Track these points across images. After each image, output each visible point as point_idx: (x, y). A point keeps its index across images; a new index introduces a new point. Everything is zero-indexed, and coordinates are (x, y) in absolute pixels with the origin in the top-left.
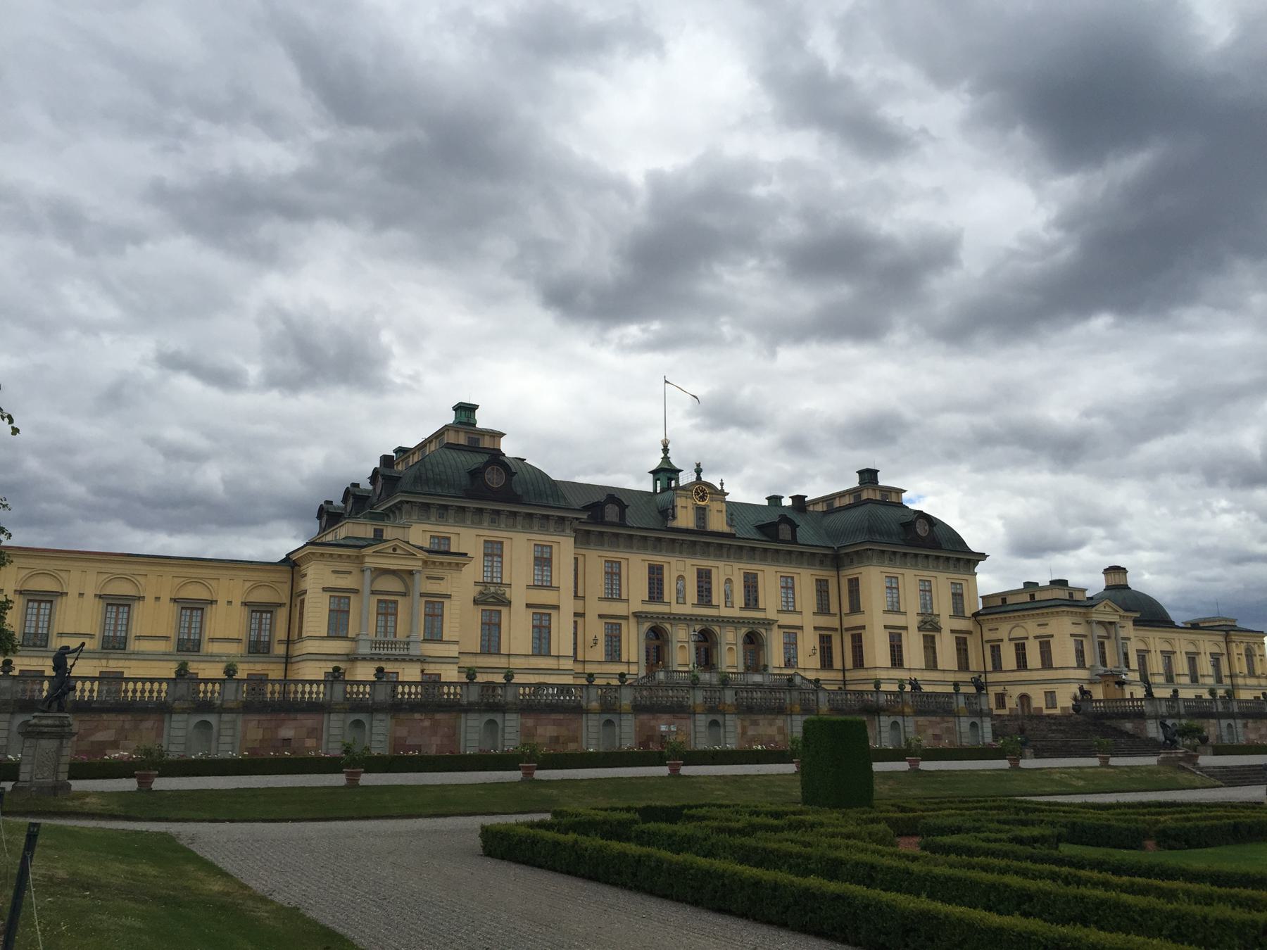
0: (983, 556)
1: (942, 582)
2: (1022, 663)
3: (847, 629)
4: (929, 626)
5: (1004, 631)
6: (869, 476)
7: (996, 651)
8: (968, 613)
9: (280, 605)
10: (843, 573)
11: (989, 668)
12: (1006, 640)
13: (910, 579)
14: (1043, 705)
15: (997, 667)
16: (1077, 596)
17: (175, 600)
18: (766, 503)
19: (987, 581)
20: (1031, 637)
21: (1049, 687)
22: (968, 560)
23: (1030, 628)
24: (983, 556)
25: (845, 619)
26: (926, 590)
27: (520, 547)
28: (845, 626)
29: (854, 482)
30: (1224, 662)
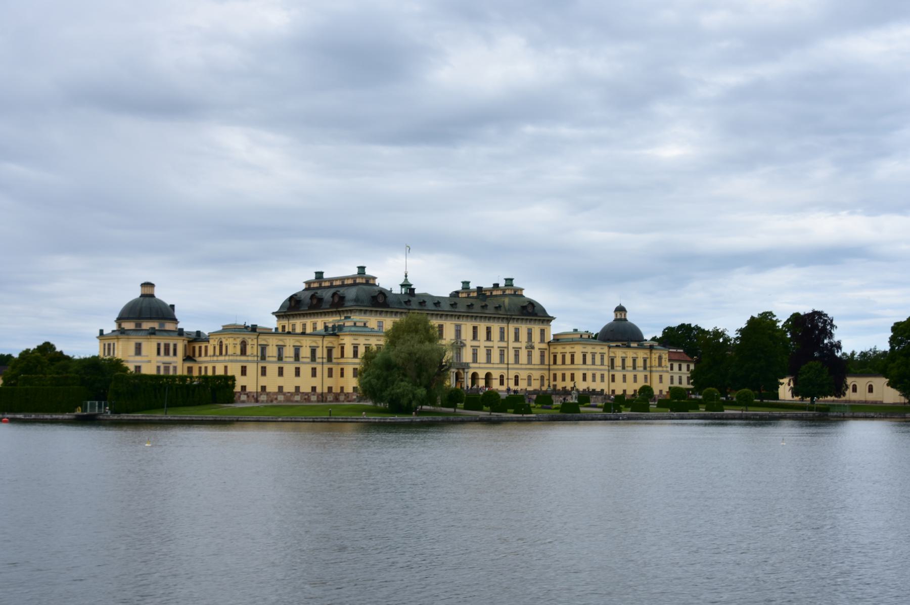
0: (553, 318)
1: (536, 329)
2: (564, 363)
4: (530, 347)
5: (559, 349)
7: (555, 357)
8: (546, 341)
11: (552, 362)
13: (524, 328)
15: (555, 363)
19: (555, 328)
22: (548, 319)
23: (568, 349)
24: (553, 318)
29: (502, 284)
30: (648, 361)
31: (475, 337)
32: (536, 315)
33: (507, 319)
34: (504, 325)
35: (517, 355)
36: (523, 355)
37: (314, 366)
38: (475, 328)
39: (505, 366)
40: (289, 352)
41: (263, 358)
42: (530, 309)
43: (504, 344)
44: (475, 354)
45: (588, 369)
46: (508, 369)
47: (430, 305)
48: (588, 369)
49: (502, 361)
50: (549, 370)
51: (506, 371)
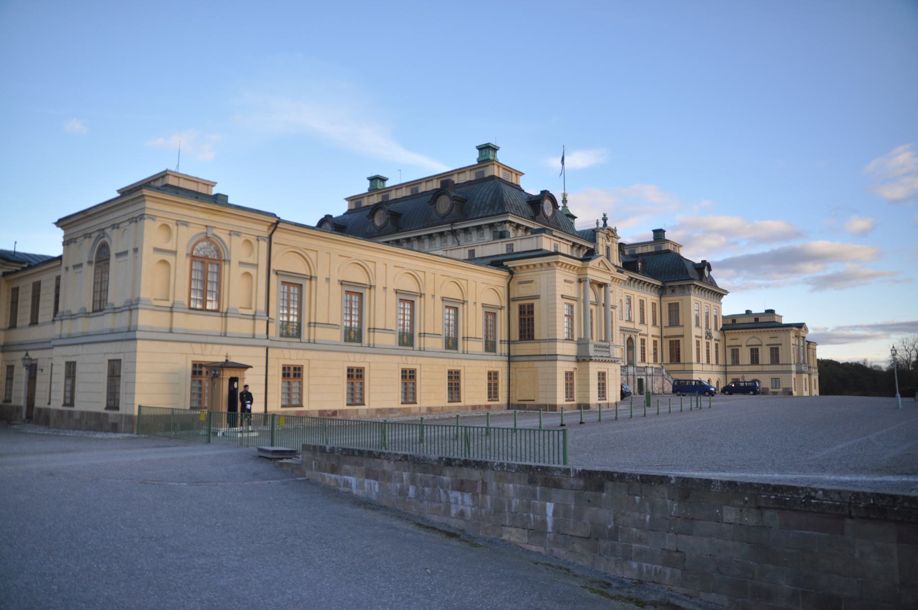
3: (665, 337)
5: (744, 340)
9: (501, 308)
10: (663, 299)
11: (729, 362)
12: (744, 345)
14: (769, 386)
15: (736, 362)
16: (777, 320)
20: (764, 344)
21: (776, 376)
23: (764, 339)
24: (727, 292)
25: (664, 330)
28: (664, 335)
29: (650, 237)
50: (726, 373)
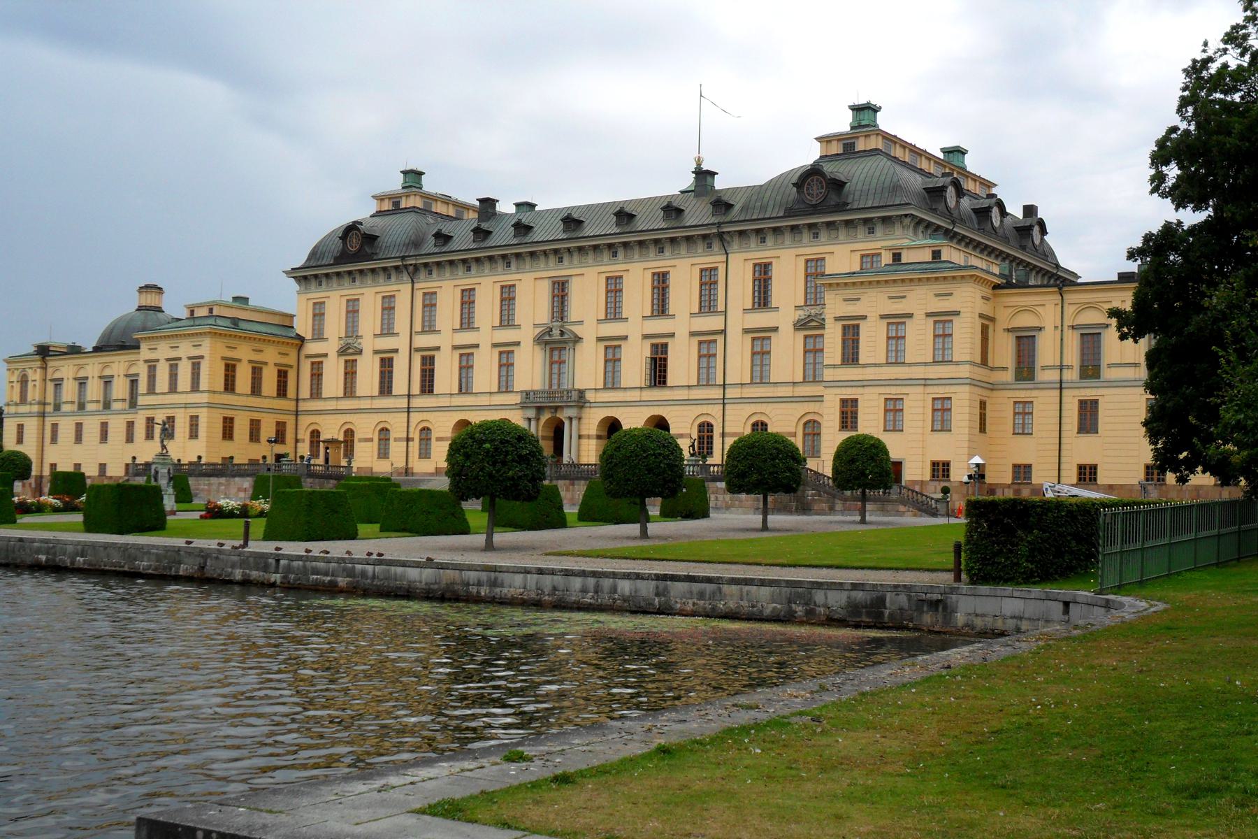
6: (865, 112)
17: (126, 376)
18: (941, 156)
26: (814, 272)
27: (370, 296)
31: (613, 312)
32: (842, 207)
33: (721, 236)
34: (713, 259)
35: (760, 355)
36: (787, 355)
37: (130, 417)
38: (614, 288)
39: (718, 393)
40: (94, 390)
41: (57, 407)
42: (816, 192)
43: (714, 323)
44: (612, 360)
45: (863, 384)
46: (724, 402)
47: (503, 235)
48: (863, 384)
49: (705, 380)
51: (716, 410)
